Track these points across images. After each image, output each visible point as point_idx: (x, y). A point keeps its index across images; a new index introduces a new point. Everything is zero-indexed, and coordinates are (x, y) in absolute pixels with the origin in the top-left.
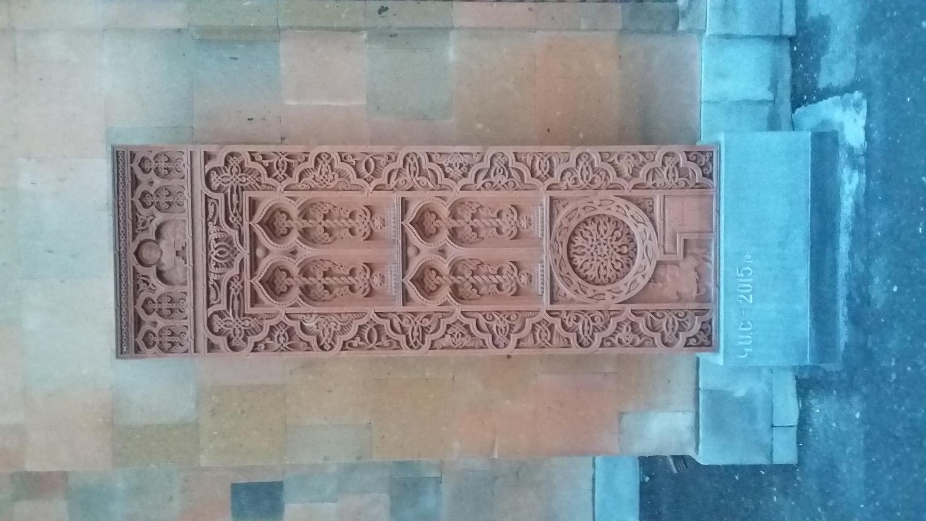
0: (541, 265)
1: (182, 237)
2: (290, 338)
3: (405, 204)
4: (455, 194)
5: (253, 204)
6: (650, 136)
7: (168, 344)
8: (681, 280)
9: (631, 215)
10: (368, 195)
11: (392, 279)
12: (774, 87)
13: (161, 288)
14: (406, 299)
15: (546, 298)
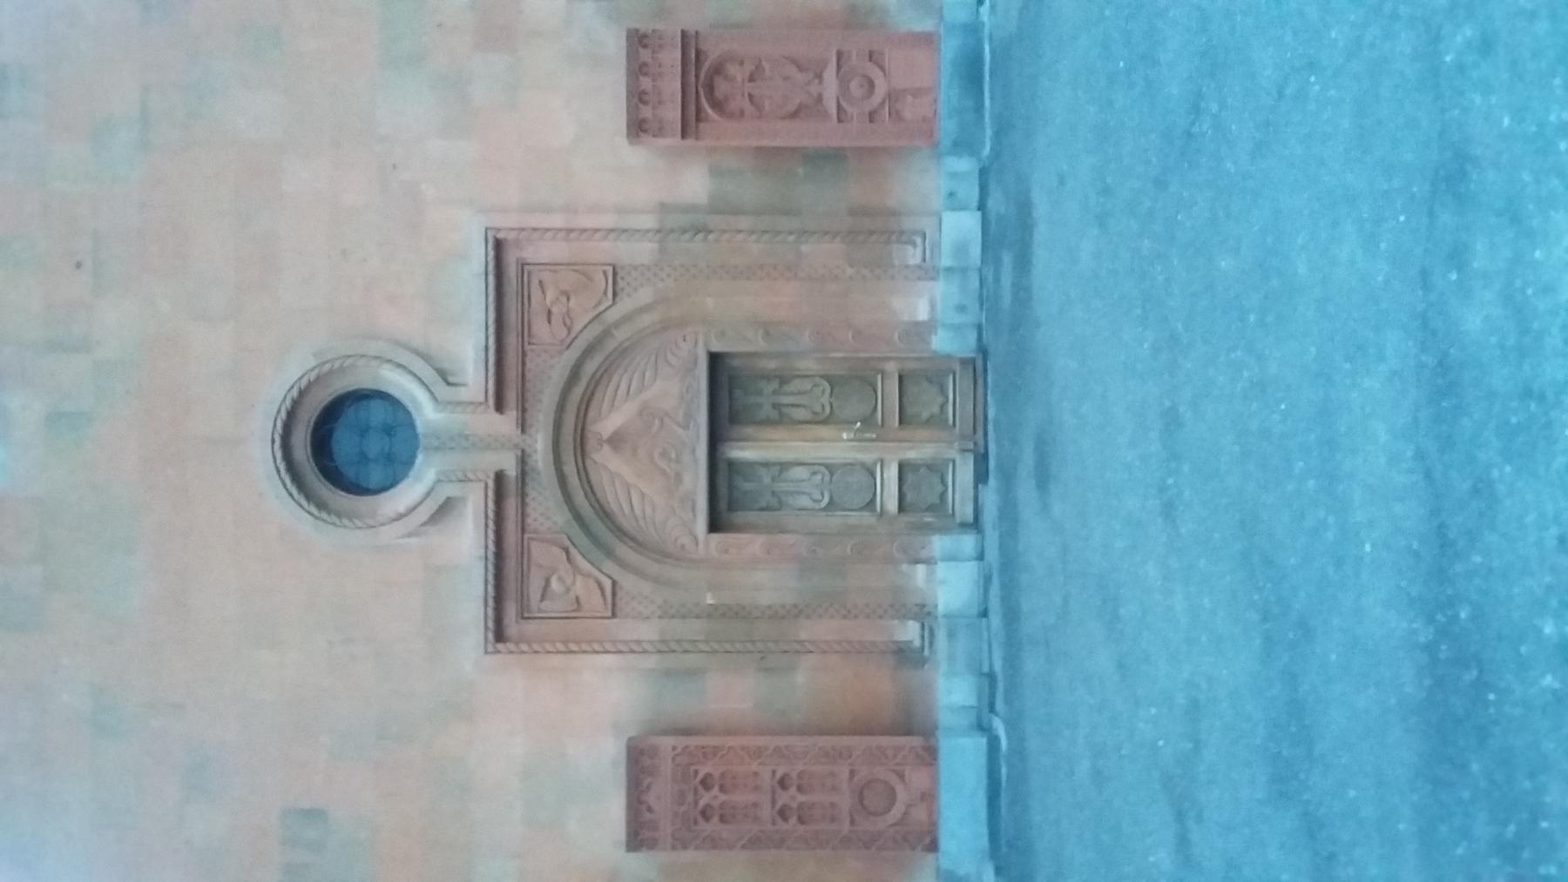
0: (845, 802)
1: (661, 794)
2: (714, 843)
3: (774, 772)
4: (800, 767)
5: (696, 772)
6: (912, 727)
7: (652, 844)
8: (919, 814)
9: (893, 779)
10: (754, 767)
11: (766, 812)
12: (979, 699)
13: (648, 816)
14: (774, 823)
15: (847, 822)
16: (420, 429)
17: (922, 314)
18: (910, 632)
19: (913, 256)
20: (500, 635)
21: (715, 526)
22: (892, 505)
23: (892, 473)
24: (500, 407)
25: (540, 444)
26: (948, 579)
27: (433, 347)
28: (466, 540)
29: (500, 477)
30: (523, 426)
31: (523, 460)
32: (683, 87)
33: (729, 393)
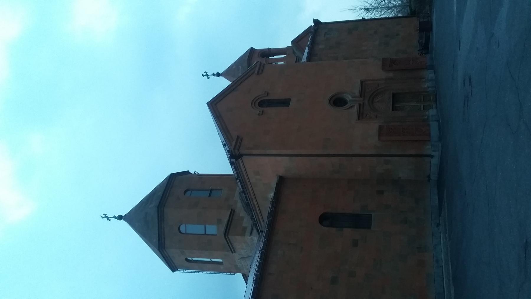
16: (348, 100)
17: (426, 86)
18: (426, 117)
19: (424, 80)
20: (359, 119)
21: (393, 110)
22: (422, 109)
23: (422, 106)
24: (361, 97)
25: (366, 102)
26: (432, 112)
27: (351, 92)
28: (355, 110)
29: (360, 104)
30: (364, 99)
31: (364, 103)
32: (389, 64)
33: (396, 98)
